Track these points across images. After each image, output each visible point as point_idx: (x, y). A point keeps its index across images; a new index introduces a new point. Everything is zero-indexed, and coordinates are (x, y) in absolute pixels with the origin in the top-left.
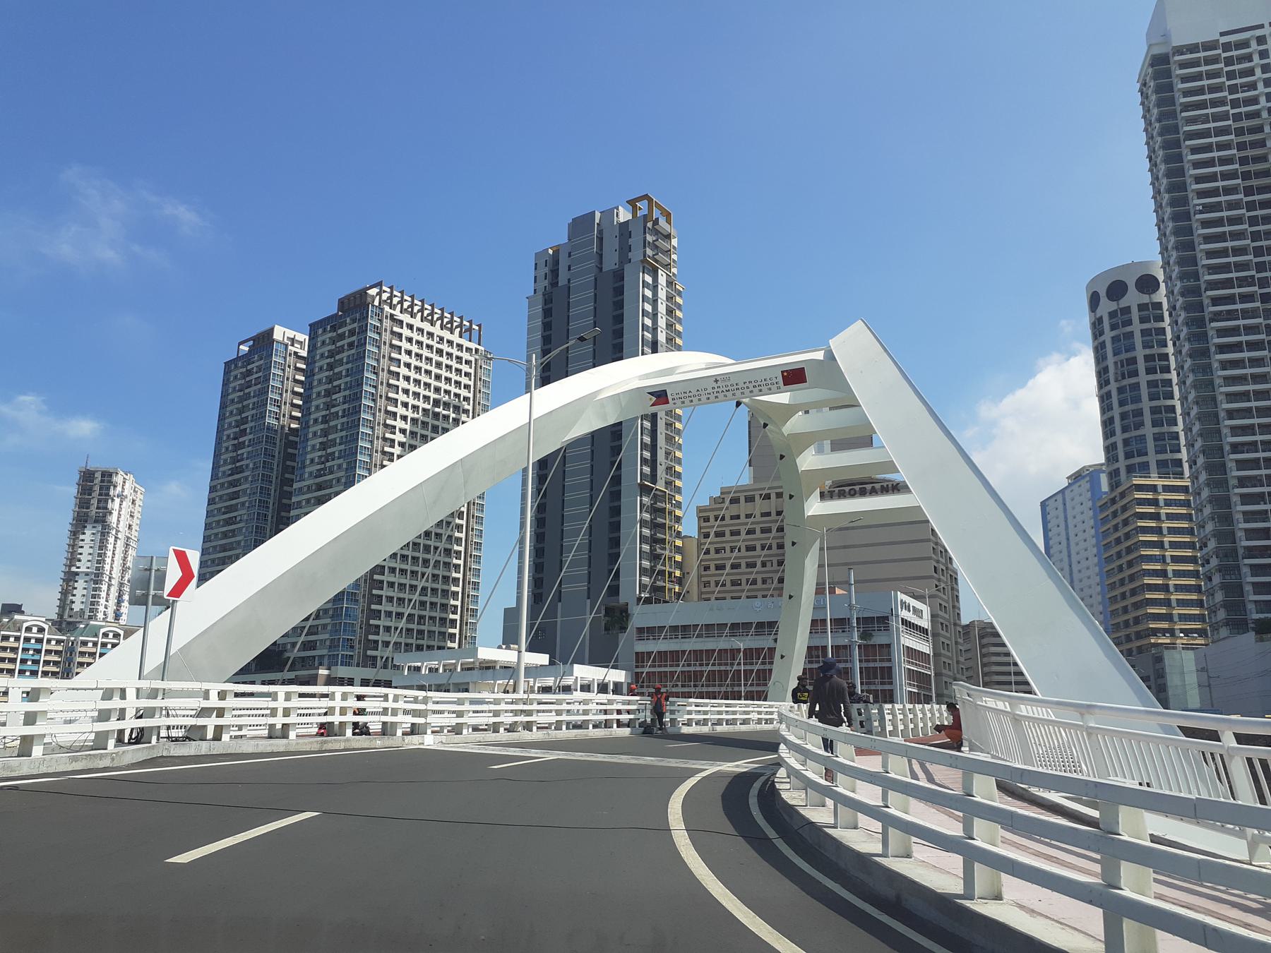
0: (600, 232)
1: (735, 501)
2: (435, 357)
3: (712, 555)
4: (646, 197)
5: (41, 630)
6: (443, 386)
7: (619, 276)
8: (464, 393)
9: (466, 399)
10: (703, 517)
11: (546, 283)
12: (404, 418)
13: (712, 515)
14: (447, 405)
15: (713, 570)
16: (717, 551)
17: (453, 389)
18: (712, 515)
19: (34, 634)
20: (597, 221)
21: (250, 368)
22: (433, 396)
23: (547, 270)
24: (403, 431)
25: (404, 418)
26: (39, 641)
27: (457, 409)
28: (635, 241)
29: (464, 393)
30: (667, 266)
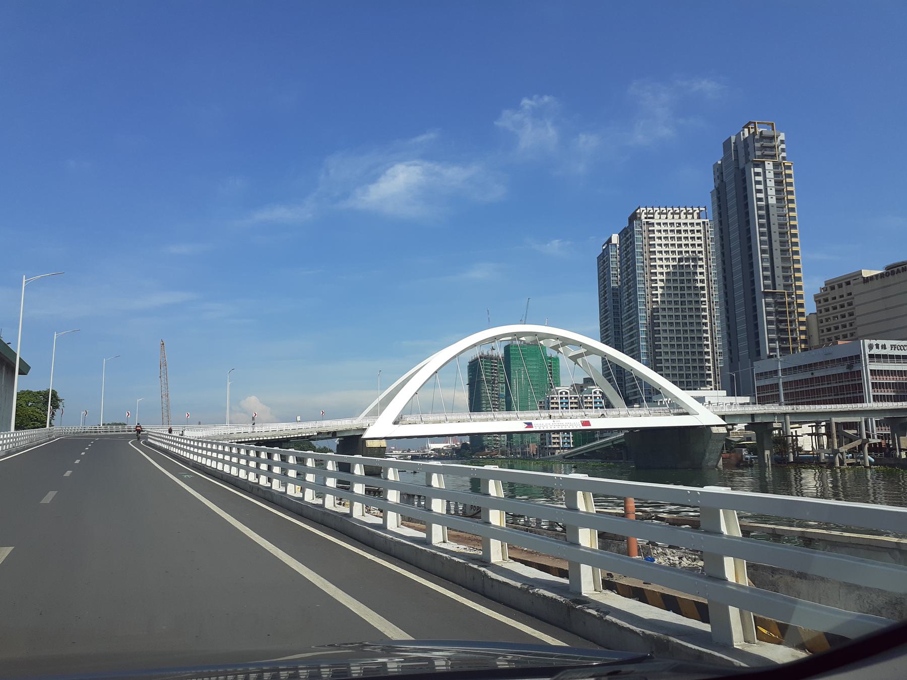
0: (736, 146)
1: (833, 288)
2: (676, 235)
3: (825, 323)
4: (750, 123)
5: (566, 393)
6: (684, 249)
7: (743, 172)
8: (698, 249)
9: (699, 252)
10: (817, 299)
11: (718, 181)
12: (662, 273)
13: (821, 299)
14: (687, 259)
15: (833, 330)
16: (827, 320)
17: (690, 249)
18: (821, 299)
19: (564, 395)
20: (733, 141)
21: (603, 260)
22: (677, 256)
23: (718, 174)
24: (662, 280)
25: (662, 273)
26: (567, 398)
27: (694, 260)
28: (750, 149)
29: (698, 249)
30: (773, 156)
